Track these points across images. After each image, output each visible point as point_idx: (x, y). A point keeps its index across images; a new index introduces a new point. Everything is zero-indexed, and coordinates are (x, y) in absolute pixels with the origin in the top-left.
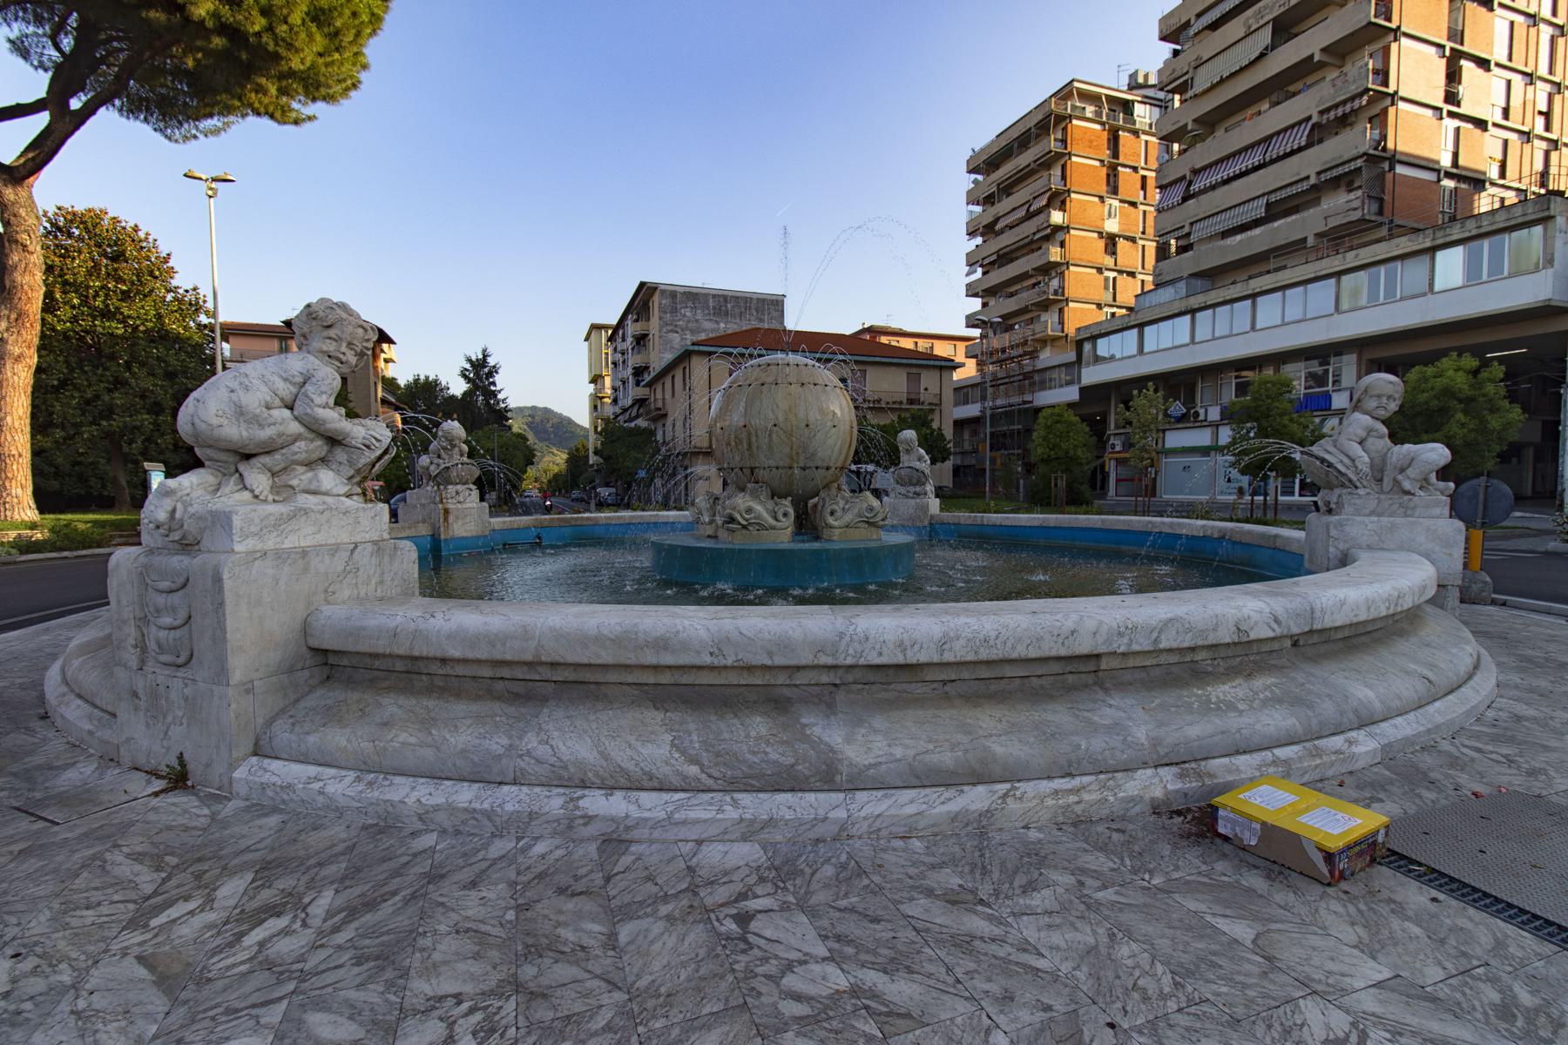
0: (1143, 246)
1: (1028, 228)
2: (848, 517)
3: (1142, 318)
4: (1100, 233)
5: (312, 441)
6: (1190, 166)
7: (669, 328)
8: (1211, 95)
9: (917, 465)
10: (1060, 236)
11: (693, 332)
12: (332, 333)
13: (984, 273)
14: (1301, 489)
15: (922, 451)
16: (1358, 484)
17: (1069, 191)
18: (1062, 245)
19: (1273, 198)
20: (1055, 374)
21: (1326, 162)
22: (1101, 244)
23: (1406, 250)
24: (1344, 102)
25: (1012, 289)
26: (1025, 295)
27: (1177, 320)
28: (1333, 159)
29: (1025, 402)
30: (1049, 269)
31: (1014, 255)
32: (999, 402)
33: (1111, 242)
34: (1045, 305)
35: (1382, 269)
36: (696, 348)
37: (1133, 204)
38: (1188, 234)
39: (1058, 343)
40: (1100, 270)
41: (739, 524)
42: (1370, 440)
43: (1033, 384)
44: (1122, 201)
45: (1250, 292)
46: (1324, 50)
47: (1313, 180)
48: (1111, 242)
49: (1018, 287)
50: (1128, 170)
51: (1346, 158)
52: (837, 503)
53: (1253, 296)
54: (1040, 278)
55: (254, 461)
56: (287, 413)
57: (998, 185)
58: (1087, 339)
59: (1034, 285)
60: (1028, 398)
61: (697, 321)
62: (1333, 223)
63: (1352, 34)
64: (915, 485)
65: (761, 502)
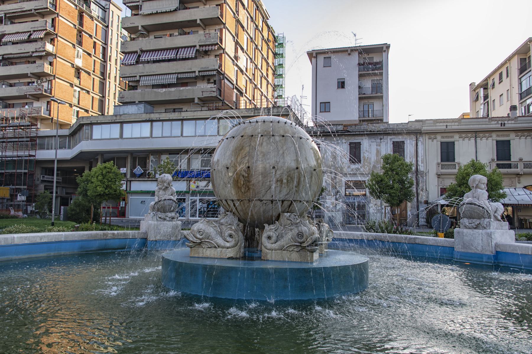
0: (94, 79)
1: (29, 48)
3: (123, 119)
4: (73, 65)
6: (140, 47)
8: (151, 17)
10: (50, 59)
14: (199, 214)
17: (56, 35)
18: (51, 64)
19: (180, 76)
20: (53, 141)
21: (202, 68)
22: (73, 71)
23: (246, 115)
24: (209, 45)
25: (12, 82)
26: (25, 88)
27: (143, 124)
28: (205, 68)
29: (30, 156)
30: (40, 76)
31: (14, 61)
33: (78, 71)
34: (37, 97)
37: (89, 55)
38: (138, 81)
39: (46, 122)
40: (72, 85)
44: (84, 51)
45: (182, 118)
46: (201, 20)
47: (197, 74)
48: (78, 71)
49: (16, 81)
50: (87, 35)
51: (210, 69)
53: (182, 120)
57: (5, 14)
58: (87, 124)
59: (29, 83)
60: (32, 153)
62: (206, 95)
63: (211, 18)
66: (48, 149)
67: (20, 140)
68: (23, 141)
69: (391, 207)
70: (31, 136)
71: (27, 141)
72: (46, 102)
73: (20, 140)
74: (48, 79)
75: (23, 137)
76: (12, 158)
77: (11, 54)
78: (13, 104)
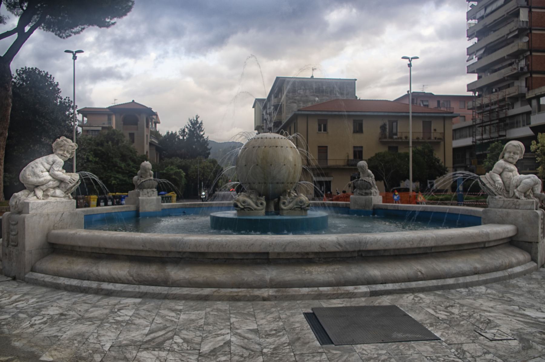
2: (291, 205)
5: (54, 181)
7: (291, 101)
9: (366, 179)
11: (304, 102)
12: (62, 148)
13: (479, 59)
15: (369, 171)
16: (496, 193)
26: (503, 71)
29: (500, 136)
32: (485, 136)
36: (300, 112)
41: (239, 207)
42: (505, 173)
43: (506, 125)
52: (286, 199)
54: (513, 60)
55: (38, 187)
56: (47, 173)
60: (502, 133)
61: (306, 96)
64: (366, 189)
65: (251, 199)
67: (493, 122)
69: (145, 188)
71: (497, 123)
72: (525, 79)
73: (493, 122)
74: (525, 56)
75: (493, 120)
77: (492, 43)
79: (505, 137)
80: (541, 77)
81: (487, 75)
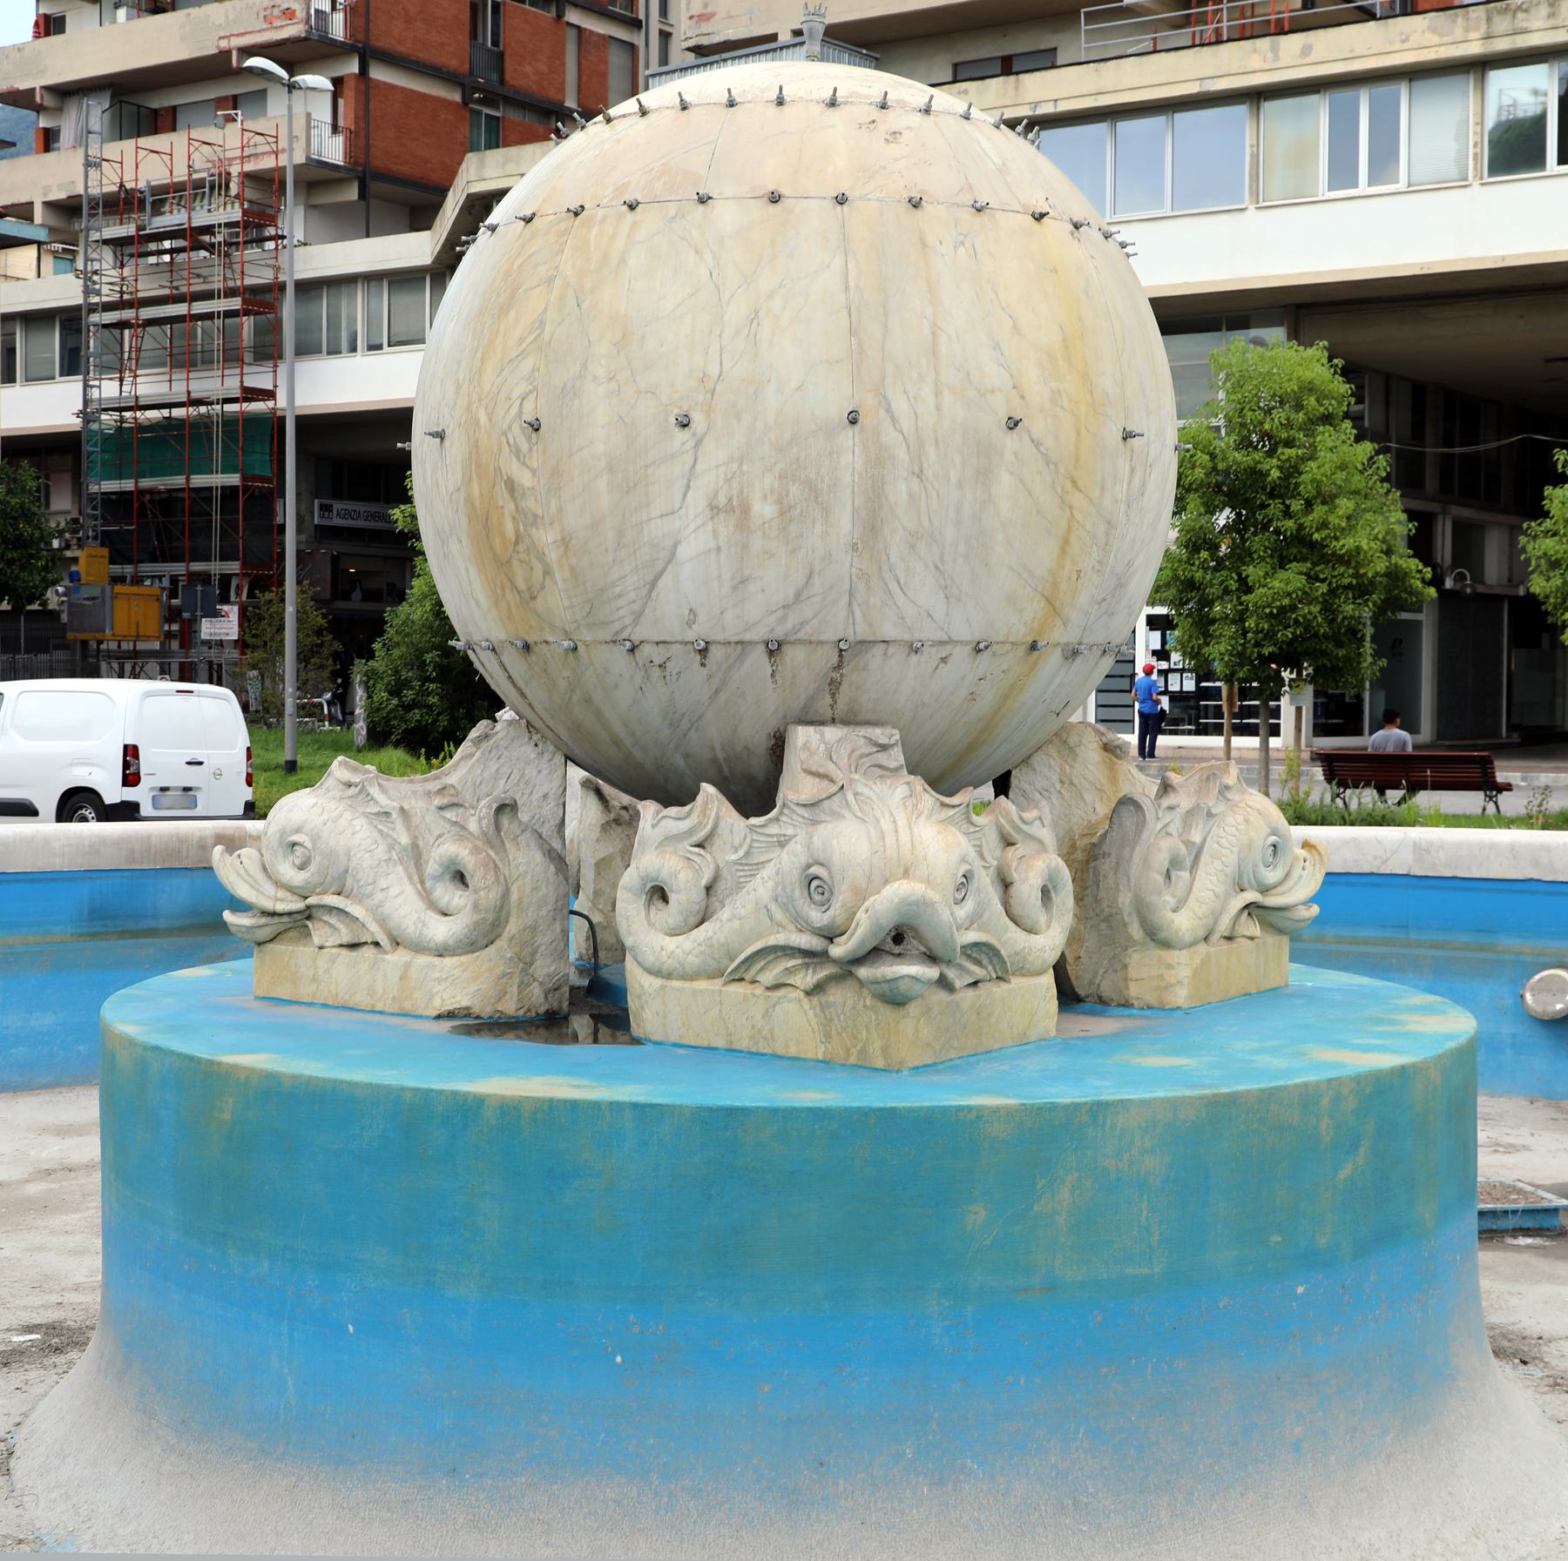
29: (250, 394)
35: (1364, 99)
60: (259, 379)
66: (334, 351)
67: (200, 307)
68: (209, 316)
70: (248, 281)
71: (229, 314)
73: (200, 307)
75: (208, 296)
76: (165, 413)
78: (174, 109)
79: (270, 404)
80: (403, 90)
81: (114, 21)
